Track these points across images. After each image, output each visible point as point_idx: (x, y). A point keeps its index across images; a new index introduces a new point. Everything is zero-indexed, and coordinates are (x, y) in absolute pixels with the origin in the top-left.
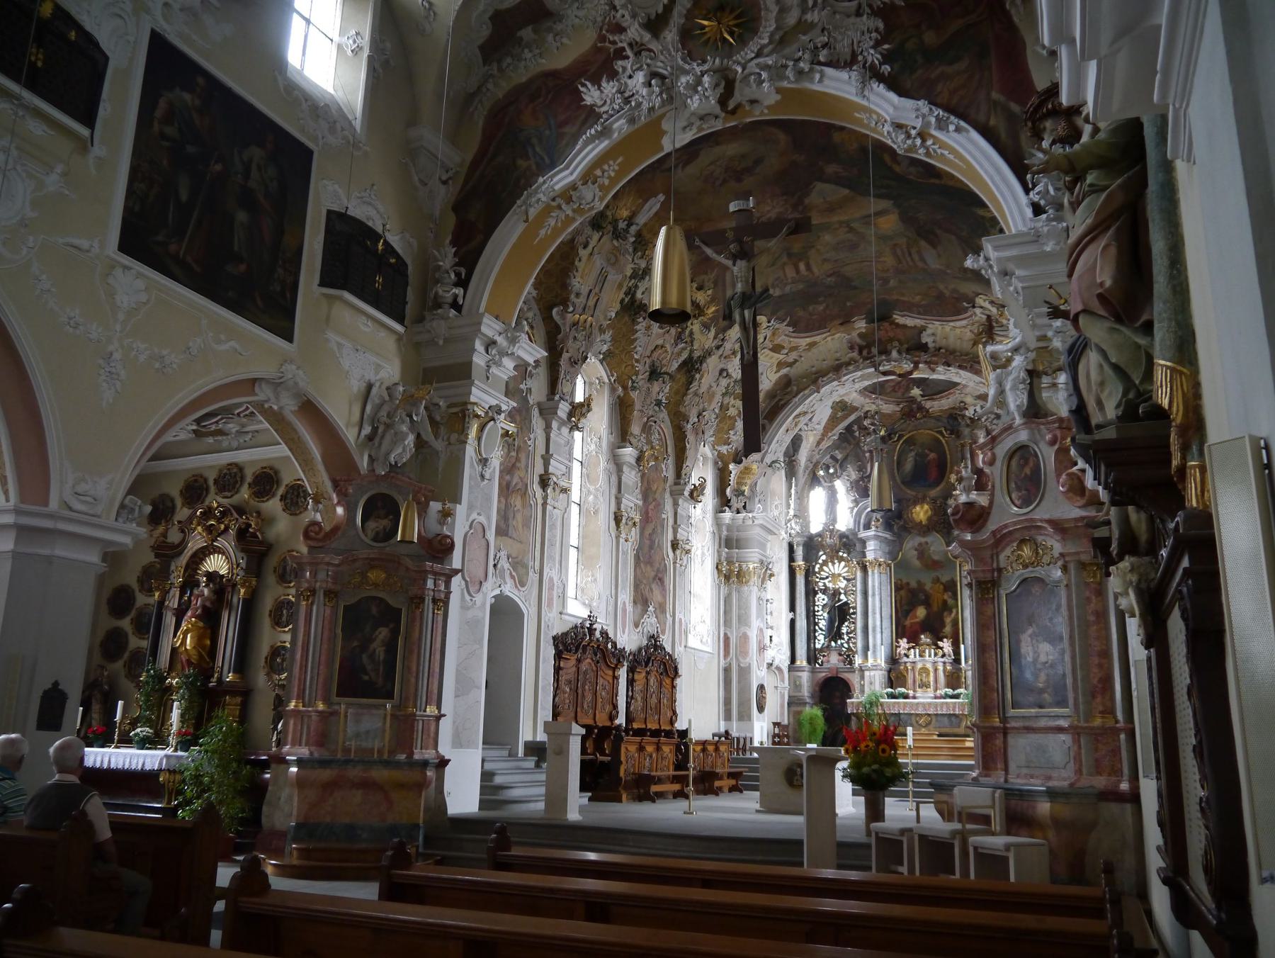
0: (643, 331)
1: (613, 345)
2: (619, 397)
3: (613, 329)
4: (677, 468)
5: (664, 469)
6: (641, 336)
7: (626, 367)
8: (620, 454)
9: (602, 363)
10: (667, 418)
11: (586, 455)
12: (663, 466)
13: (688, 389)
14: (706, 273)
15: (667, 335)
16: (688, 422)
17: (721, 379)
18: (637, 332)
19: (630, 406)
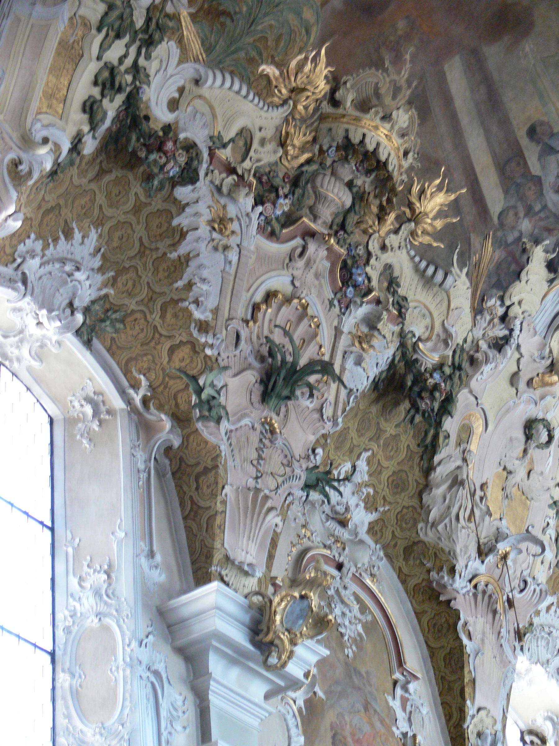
0: (204, 230)
1: (113, 282)
2: (168, 450)
3: (99, 223)
4: (448, 717)
5: (400, 714)
6: (202, 246)
7: (172, 351)
8: (185, 612)
9: (88, 344)
10: (384, 563)
11: (68, 630)
12: (396, 704)
13: (429, 470)
14: (379, 64)
15: (301, 263)
16: (452, 571)
17: (533, 452)
18: (183, 235)
19: (206, 470)
